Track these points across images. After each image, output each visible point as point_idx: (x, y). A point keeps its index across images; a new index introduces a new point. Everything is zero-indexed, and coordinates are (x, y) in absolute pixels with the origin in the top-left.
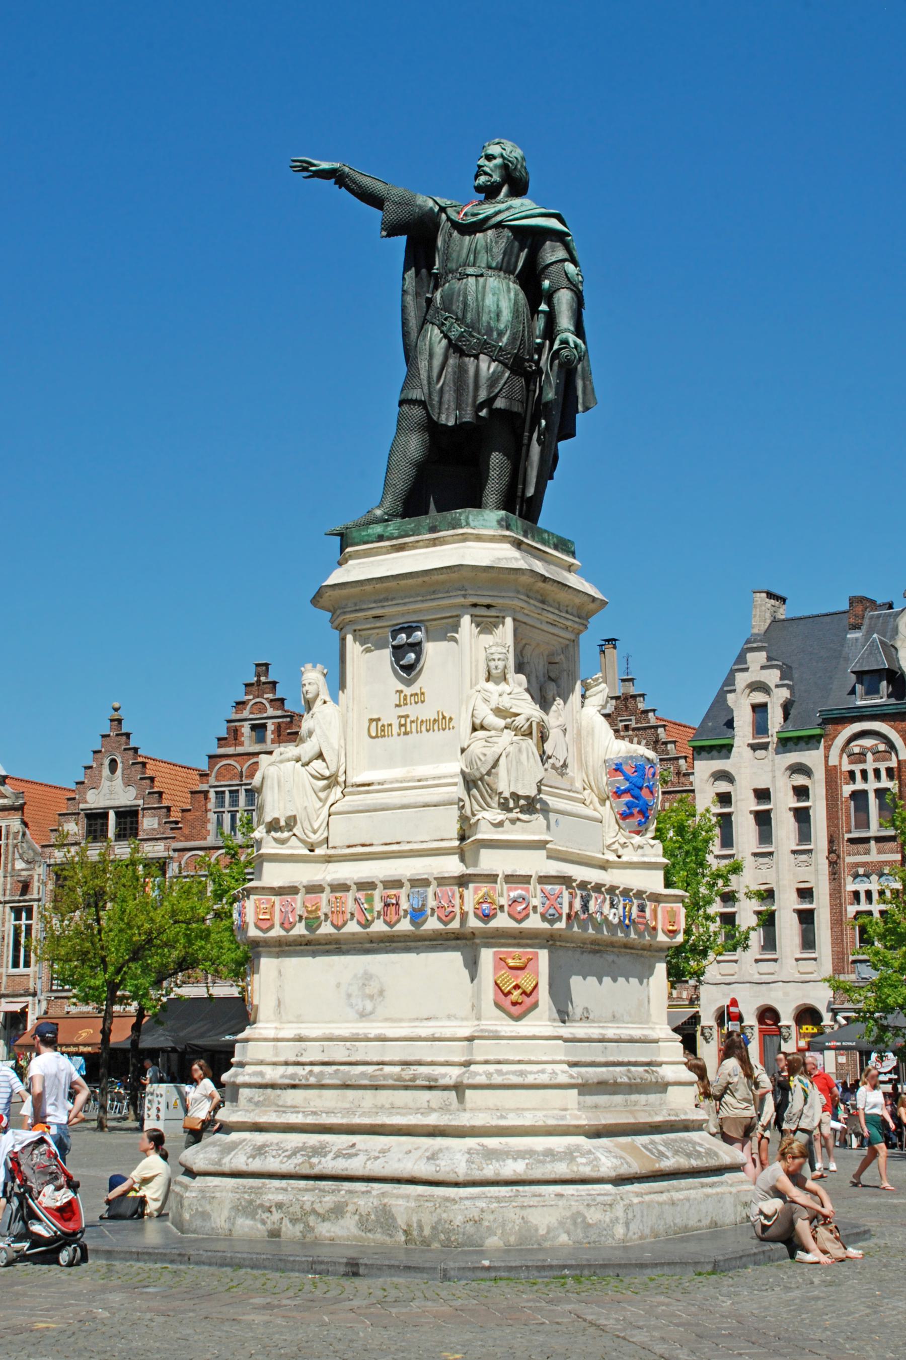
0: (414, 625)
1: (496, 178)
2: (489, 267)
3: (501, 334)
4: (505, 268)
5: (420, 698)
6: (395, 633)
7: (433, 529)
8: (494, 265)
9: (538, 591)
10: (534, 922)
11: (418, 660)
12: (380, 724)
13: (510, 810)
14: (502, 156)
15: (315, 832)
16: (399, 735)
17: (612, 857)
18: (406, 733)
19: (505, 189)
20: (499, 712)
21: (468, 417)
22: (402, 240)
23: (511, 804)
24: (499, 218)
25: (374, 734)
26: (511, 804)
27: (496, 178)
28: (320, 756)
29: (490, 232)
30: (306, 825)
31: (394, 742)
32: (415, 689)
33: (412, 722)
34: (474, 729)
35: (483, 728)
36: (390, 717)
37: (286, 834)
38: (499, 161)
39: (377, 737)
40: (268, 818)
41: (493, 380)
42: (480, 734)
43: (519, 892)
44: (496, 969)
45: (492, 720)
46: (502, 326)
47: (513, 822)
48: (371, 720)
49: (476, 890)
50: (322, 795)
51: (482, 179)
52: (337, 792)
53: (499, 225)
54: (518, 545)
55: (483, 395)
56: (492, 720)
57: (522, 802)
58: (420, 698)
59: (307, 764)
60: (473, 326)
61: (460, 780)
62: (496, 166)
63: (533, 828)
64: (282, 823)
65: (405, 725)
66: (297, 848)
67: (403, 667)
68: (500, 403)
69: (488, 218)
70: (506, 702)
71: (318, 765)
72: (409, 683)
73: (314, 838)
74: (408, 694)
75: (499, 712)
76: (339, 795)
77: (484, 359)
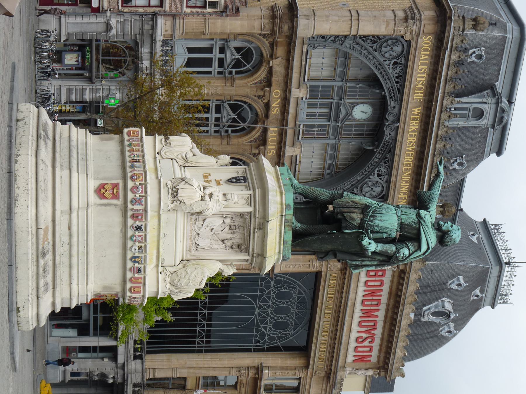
1: (444, 228)
2: (401, 219)
3: (372, 221)
4: (402, 226)
8: (403, 221)
10: (130, 196)
13: (172, 190)
15: (165, 153)
17: (160, 269)
19: (440, 234)
23: (174, 189)
24: (422, 222)
26: (174, 189)
27: (444, 228)
29: (417, 220)
30: (168, 150)
37: (163, 143)
38: (450, 229)
41: (353, 219)
43: (141, 190)
45: (208, 191)
46: (375, 222)
47: (168, 191)
48: (210, 174)
49: (142, 174)
50: (180, 156)
52: (181, 162)
53: (420, 223)
55: (346, 215)
56: (208, 191)
57: (175, 194)
61: (184, 176)
62: (448, 228)
64: (168, 141)
66: (158, 147)
70: (215, 197)
75: (211, 196)
76: (180, 164)
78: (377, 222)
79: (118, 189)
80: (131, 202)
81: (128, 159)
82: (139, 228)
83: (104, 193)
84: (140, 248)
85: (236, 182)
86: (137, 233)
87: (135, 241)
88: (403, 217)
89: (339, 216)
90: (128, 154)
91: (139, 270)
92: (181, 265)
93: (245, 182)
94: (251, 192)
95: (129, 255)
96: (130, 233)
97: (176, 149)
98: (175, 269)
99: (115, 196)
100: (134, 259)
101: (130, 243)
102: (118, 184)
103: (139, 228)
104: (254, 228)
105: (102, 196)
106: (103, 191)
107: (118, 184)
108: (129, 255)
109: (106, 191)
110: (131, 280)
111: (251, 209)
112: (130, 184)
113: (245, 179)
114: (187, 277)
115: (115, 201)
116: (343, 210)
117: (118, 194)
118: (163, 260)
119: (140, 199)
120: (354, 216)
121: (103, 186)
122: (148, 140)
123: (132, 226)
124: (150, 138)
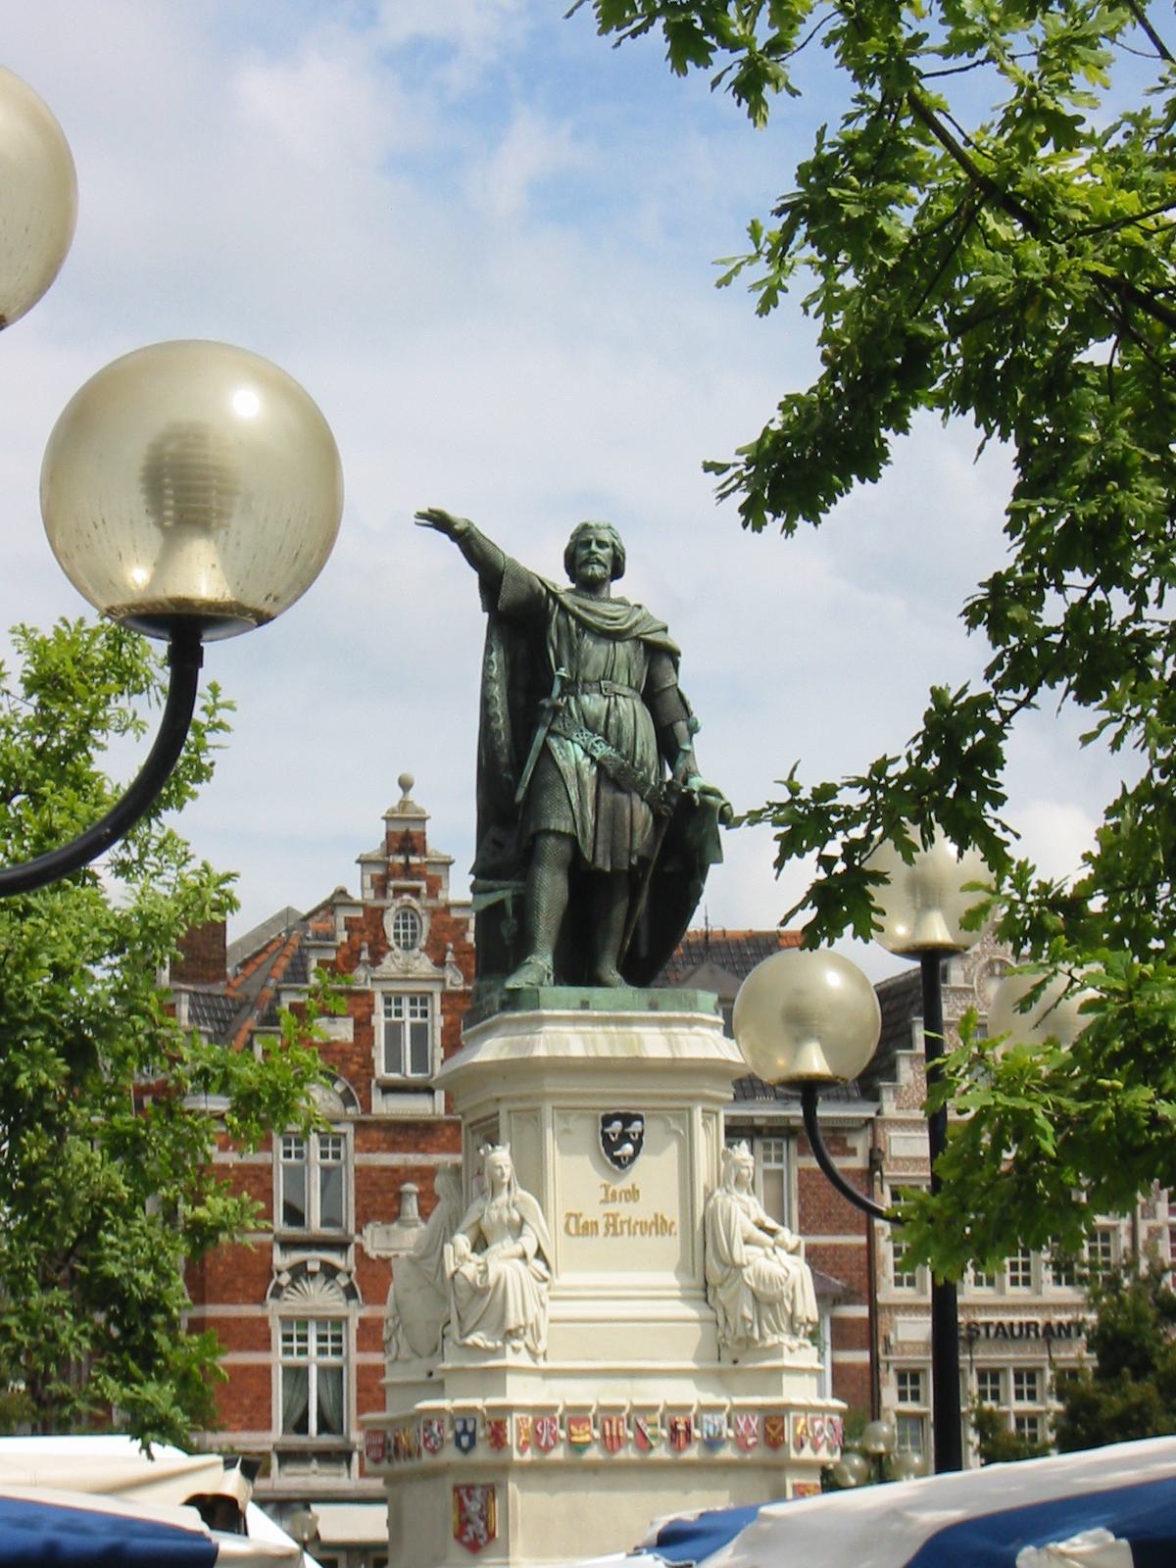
0: (633, 1112)
5: (633, 1194)
6: (607, 1120)
7: (653, 1007)
11: (637, 1152)
12: (582, 1221)
14: (613, 545)
16: (606, 1235)
18: (615, 1234)
25: (573, 1231)
29: (628, 643)
31: (599, 1243)
32: (624, 1184)
33: (622, 1223)
36: (594, 1213)
39: (578, 1234)
48: (569, 1215)
53: (637, 639)
58: (633, 1194)
65: (614, 1225)
67: (617, 1160)
71: (540, 1265)
72: (618, 1176)
74: (618, 1190)
81: (661, 1453)
85: (638, 1146)
93: (640, 1118)
113: (627, 1119)
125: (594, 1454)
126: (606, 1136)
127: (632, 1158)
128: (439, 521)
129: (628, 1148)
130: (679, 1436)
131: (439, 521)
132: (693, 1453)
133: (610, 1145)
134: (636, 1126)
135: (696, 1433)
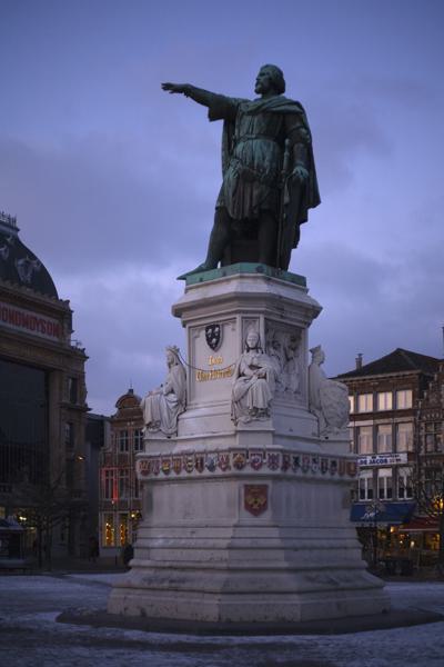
3: (264, 170)
9: (276, 302)
10: (265, 470)
20: (252, 367)
21: (246, 214)
22: (221, 122)
27: (266, 85)
28: (172, 392)
34: (240, 376)
35: (244, 375)
40: (147, 422)
41: (260, 195)
42: (243, 378)
44: (246, 494)
45: (248, 372)
49: (235, 455)
51: (259, 86)
54: (268, 280)
56: (248, 372)
59: (167, 395)
60: (251, 165)
63: (267, 425)
67: (211, 346)
68: (265, 207)
69: (259, 107)
70: (255, 362)
73: (170, 431)
75: (252, 367)
77: (256, 183)
78: (267, 164)
79: (252, 486)
80: (273, 469)
81: (195, 473)
82: (297, 460)
83: (260, 505)
84: (314, 460)
85: (218, 338)
86: (301, 463)
87: (308, 467)
88: (256, 131)
89: (255, 212)
90: (184, 474)
91: (334, 463)
92: (318, 413)
93: (218, 326)
94: (238, 317)
95: (319, 475)
96: (299, 473)
97: (165, 414)
98: (323, 422)
99: (263, 489)
100: (324, 470)
101: (309, 474)
102: (246, 486)
103: (297, 460)
104: (282, 317)
105: (263, 508)
106: (255, 507)
107: (246, 486)
108: (319, 475)
109: (256, 502)
110: (341, 474)
111: (262, 320)
112: (248, 470)
113: (213, 327)
114: (335, 405)
115: (270, 491)
116: (247, 206)
117: (259, 486)
118: (314, 434)
119: (270, 457)
120: (256, 193)
121: (249, 507)
122: (151, 450)
123: (294, 470)
124: (147, 446)
125: (173, 475)
126: (207, 336)
127: (217, 343)
128: (167, 87)
129: (214, 340)
130: (200, 466)
131: (167, 87)
132: (206, 472)
133: (209, 340)
134: (217, 329)
135: (206, 463)
